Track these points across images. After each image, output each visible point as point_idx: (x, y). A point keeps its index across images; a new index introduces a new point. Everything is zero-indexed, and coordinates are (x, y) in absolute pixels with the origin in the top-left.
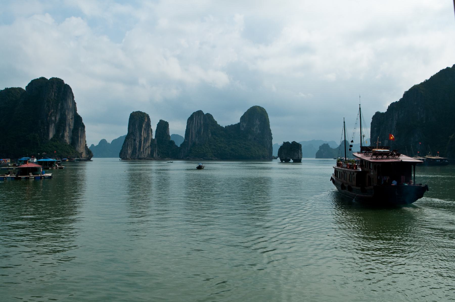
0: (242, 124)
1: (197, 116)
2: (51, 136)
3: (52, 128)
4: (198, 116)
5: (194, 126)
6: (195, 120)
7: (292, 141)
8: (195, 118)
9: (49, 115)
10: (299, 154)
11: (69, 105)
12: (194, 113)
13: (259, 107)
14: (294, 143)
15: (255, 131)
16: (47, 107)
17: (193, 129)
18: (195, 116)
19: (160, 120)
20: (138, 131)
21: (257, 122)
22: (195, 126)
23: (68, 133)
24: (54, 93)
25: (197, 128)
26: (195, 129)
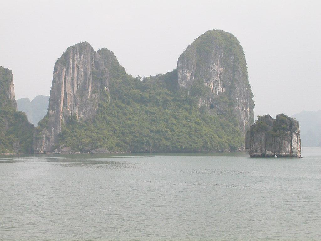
0: (181, 71)
1: (78, 57)
4: (80, 56)
5: (69, 78)
6: (73, 64)
7: (278, 114)
8: (73, 60)
10: (294, 144)
12: (69, 49)
13: (221, 32)
14: (282, 119)
15: (211, 88)
17: (68, 85)
18: (71, 56)
21: (218, 68)
22: (73, 80)
25: (78, 82)
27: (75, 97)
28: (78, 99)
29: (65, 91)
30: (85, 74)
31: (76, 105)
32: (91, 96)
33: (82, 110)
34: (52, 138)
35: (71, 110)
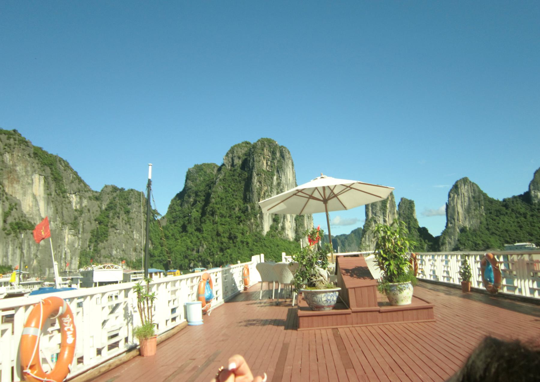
1: (463, 187)
2: (266, 228)
3: (267, 217)
4: (464, 186)
8: (461, 189)
9: (262, 196)
11: (288, 179)
16: (258, 184)
19: (402, 199)
20: (381, 215)
23: (290, 222)
24: (266, 161)
26: (462, 206)
27: (464, 214)
28: (467, 215)
29: (457, 210)
30: (469, 198)
31: (466, 219)
32: (474, 213)
33: (470, 222)
34: (453, 243)
35: (462, 223)
